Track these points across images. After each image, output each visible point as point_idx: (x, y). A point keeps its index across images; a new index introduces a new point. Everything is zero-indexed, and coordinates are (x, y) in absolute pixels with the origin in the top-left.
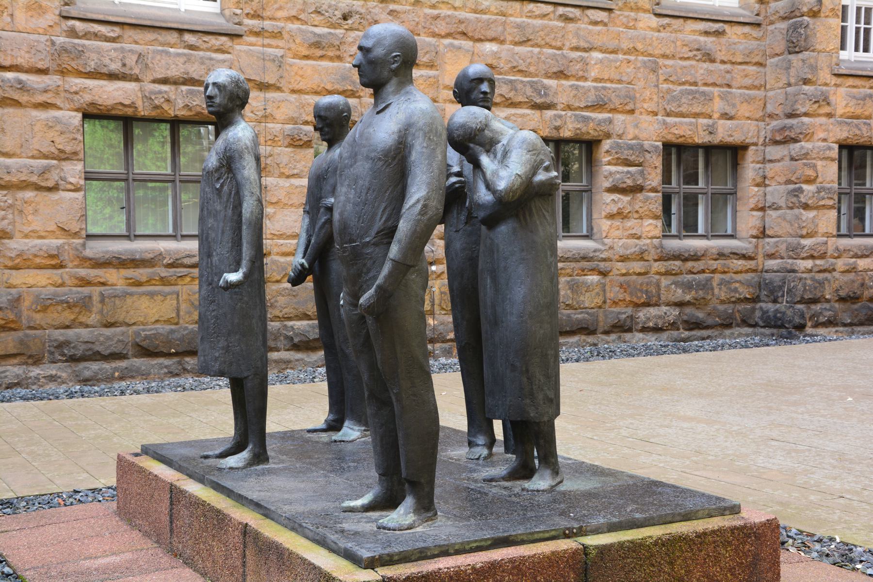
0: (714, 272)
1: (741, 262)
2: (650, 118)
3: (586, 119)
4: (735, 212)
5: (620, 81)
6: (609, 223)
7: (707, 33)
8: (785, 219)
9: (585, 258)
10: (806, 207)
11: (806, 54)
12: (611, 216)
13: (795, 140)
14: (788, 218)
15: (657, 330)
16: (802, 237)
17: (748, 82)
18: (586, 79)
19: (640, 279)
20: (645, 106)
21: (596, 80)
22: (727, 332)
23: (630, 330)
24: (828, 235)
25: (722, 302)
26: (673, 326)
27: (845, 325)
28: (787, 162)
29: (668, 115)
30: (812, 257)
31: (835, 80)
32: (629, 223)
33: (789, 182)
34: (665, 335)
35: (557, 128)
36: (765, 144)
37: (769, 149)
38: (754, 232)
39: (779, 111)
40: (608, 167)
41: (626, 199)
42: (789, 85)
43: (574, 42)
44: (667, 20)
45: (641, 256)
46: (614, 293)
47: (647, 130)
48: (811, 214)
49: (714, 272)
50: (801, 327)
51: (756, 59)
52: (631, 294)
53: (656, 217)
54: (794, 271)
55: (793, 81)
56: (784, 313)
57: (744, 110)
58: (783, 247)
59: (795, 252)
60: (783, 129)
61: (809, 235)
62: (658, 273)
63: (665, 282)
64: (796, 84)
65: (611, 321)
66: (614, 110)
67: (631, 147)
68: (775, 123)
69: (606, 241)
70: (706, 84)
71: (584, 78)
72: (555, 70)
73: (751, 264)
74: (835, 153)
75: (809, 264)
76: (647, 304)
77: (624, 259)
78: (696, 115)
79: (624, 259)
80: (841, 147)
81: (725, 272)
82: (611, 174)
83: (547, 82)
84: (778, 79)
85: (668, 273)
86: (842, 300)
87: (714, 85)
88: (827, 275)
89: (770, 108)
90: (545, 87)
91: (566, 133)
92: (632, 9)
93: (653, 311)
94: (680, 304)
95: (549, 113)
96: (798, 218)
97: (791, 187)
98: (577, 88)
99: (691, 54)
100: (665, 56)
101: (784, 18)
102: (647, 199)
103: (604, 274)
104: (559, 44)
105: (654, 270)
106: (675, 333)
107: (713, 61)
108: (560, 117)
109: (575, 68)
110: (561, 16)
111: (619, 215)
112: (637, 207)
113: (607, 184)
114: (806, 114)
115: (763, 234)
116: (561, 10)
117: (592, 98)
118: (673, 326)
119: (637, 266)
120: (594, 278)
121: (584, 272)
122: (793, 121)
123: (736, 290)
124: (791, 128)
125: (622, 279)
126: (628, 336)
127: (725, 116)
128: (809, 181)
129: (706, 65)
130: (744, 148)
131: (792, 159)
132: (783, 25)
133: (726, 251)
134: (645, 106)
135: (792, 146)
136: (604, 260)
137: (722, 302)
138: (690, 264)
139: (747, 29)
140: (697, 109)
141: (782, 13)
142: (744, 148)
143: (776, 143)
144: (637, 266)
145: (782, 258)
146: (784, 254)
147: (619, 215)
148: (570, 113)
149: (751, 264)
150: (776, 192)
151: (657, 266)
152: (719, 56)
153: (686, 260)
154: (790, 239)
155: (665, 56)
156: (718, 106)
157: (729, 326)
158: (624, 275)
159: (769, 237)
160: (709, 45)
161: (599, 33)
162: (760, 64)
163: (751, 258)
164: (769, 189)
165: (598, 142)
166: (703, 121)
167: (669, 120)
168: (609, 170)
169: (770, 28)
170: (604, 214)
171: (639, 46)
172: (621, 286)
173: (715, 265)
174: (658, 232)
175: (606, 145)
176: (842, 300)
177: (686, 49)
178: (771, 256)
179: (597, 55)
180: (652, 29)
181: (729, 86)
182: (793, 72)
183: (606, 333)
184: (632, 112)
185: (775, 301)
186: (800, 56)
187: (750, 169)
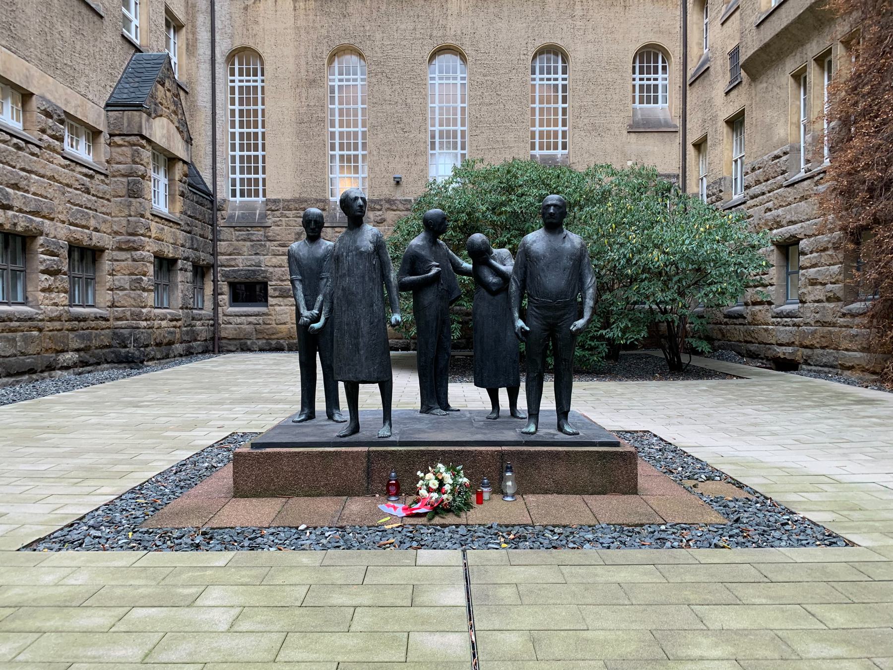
0: (93, 328)
1: (104, 323)
2: (61, 225)
3: (31, 220)
4: (95, 291)
5: (46, 197)
6: (43, 294)
7: (86, 175)
8: (130, 297)
9: (31, 319)
10: (144, 290)
11: (141, 200)
12: (43, 290)
13: (136, 249)
14: (133, 296)
15: (67, 368)
16: (142, 307)
17: (104, 209)
18: (29, 193)
19: (59, 334)
20: (60, 216)
21: (34, 194)
22: (99, 367)
23: (54, 369)
24: (151, 307)
25: (96, 348)
26: (75, 365)
27: (158, 359)
28: (130, 262)
29: (70, 224)
30: (146, 320)
31: (151, 217)
32: (53, 295)
33: (132, 274)
34: (71, 371)
35: (15, 224)
36: (112, 250)
37: (114, 253)
38: (109, 304)
39: (123, 231)
40: (42, 256)
41: (52, 278)
42: (130, 216)
43: (23, 165)
44: (68, 162)
45: (59, 319)
46: (48, 344)
47: (58, 232)
48: (145, 294)
49: (93, 328)
50: (142, 362)
51: (108, 197)
52: (56, 344)
53: (65, 292)
54: (138, 328)
55: (133, 214)
56: (133, 354)
57: (103, 227)
58: (129, 313)
59: (138, 317)
60: (129, 241)
61: (145, 307)
62: (67, 330)
63: (71, 335)
64: (135, 216)
65: (46, 364)
66: (44, 217)
67: (54, 243)
68: (118, 238)
69: (42, 307)
70: (86, 208)
71: (27, 191)
72: (13, 182)
73: (107, 324)
74: (152, 259)
75: (144, 324)
76: (63, 351)
77: (51, 320)
78: (83, 227)
79: (51, 320)
80: (155, 257)
81: (97, 329)
82: (44, 260)
83: (7, 189)
84: (120, 211)
85: (72, 330)
86: (157, 345)
87: (90, 209)
88: (151, 330)
89: (115, 228)
90: (7, 193)
91: (19, 229)
92: (51, 150)
93: (68, 356)
94: (77, 350)
95: (10, 213)
96: (140, 296)
97: (134, 277)
98: (25, 197)
99: (79, 187)
100: (68, 185)
101: (123, 176)
102: (63, 279)
103: (40, 330)
104: (14, 164)
105: (65, 327)
106: (76, 370)
107: (89, 194)
108: (17, 216)
109: (23, 183)
110: (15, 144)
111: (48, 290)
112: (57, 284)
113: (42, 268)
114: (142, 235)
115: (113, 306)
116: (15, 140)
117: (32, 207)
118: (75, 365)
119: (57, 325)
120: (35, 333)
121: (30, 329)
122: (136, 238)
123: (102, 340)
124: (134, 241)
125: (50, 333)
126: (53, 373)
127: (96, 230)
128: (145, 275)
129: (86, 195)
130: (102, 250)
131: (134, 260)
132: (124, 180)
133: (98, 316)
134: (60, 216)
135: (133, 253)
136: (41, 320)
137: (96, 348)
138: (82, 323)
139: (103, 177)
140: (84, 223)
141: (123, 172)
142: (102, 250)
143: (120, 249)
144: (57, 325)
145: (127, 320)
146: (129, 318)
147: (48, 290)
148: (21, 215)
149: (107, 324)
150: (123, 279)
151: (68, 325)
152: (92, 192)
153: (79, 321)
154: (133, 309)
155: (68, 185)
156: (93, 223)
157: (99, 364)
158: (50, 331)
159: (117, 307)
160: (88, 183)
161: (35, 162)
162: (108, 200)
163: (108, 320)
164: (115, 277)
165: (34, 237)
166: (87, 231)
167: (71, 227)
168: (43, 259)
169: (113, 179)
170: (40, 288)
171: (56, 176)
172: (50, 338)
173: (93, 324)
174: (67, 302)
175: (41, 240)
176: (157, 345)
177: (77, 183)
178: (117, 319)
179: (33, 176)
180: (61, 166)
181: (96, 211)
182: (133, 208)
183: (42, 372)
184: (52, 219)
185: (126, 347)
186: (138, 200)
187: (106, 265)
